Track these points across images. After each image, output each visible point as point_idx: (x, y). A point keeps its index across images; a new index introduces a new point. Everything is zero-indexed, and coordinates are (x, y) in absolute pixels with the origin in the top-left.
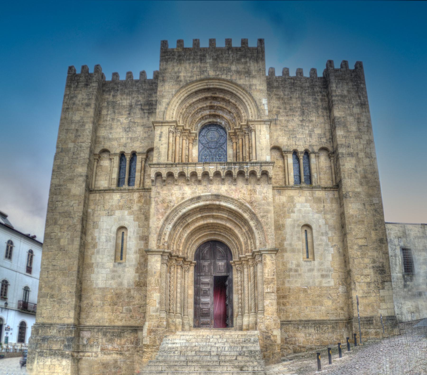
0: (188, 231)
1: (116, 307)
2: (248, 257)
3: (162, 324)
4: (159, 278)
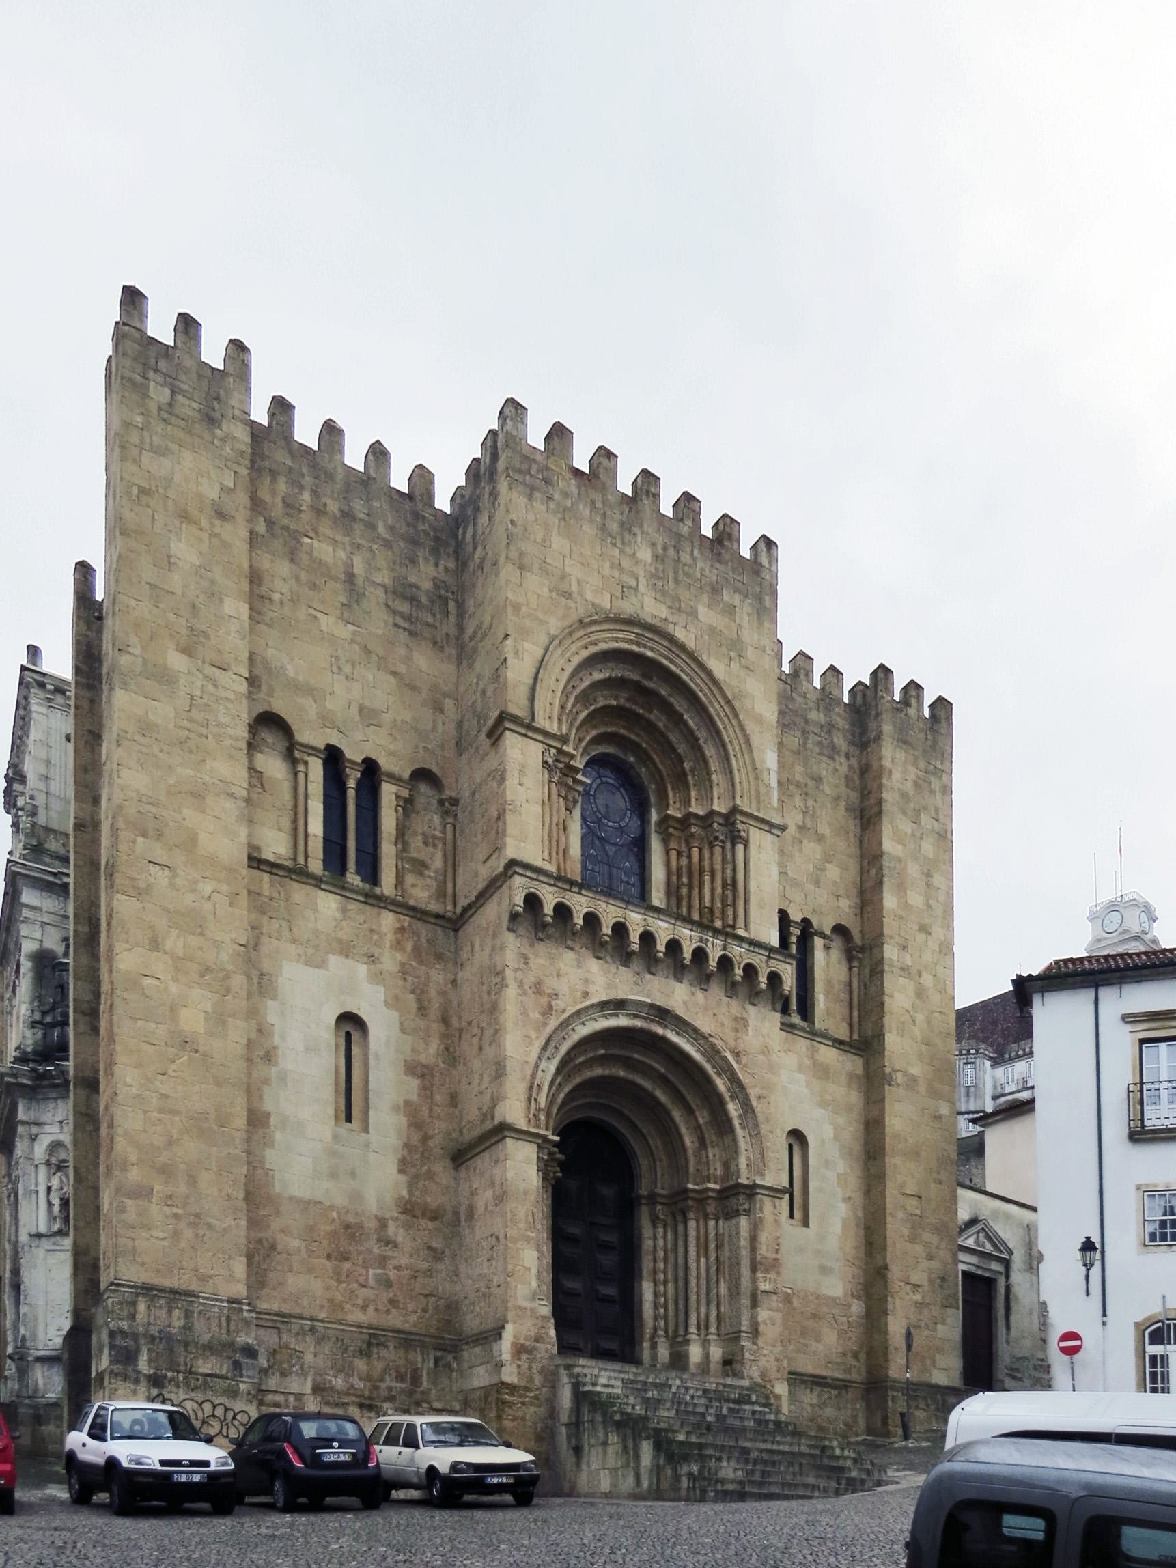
1: (347, 1266)
2: (710, 1194)
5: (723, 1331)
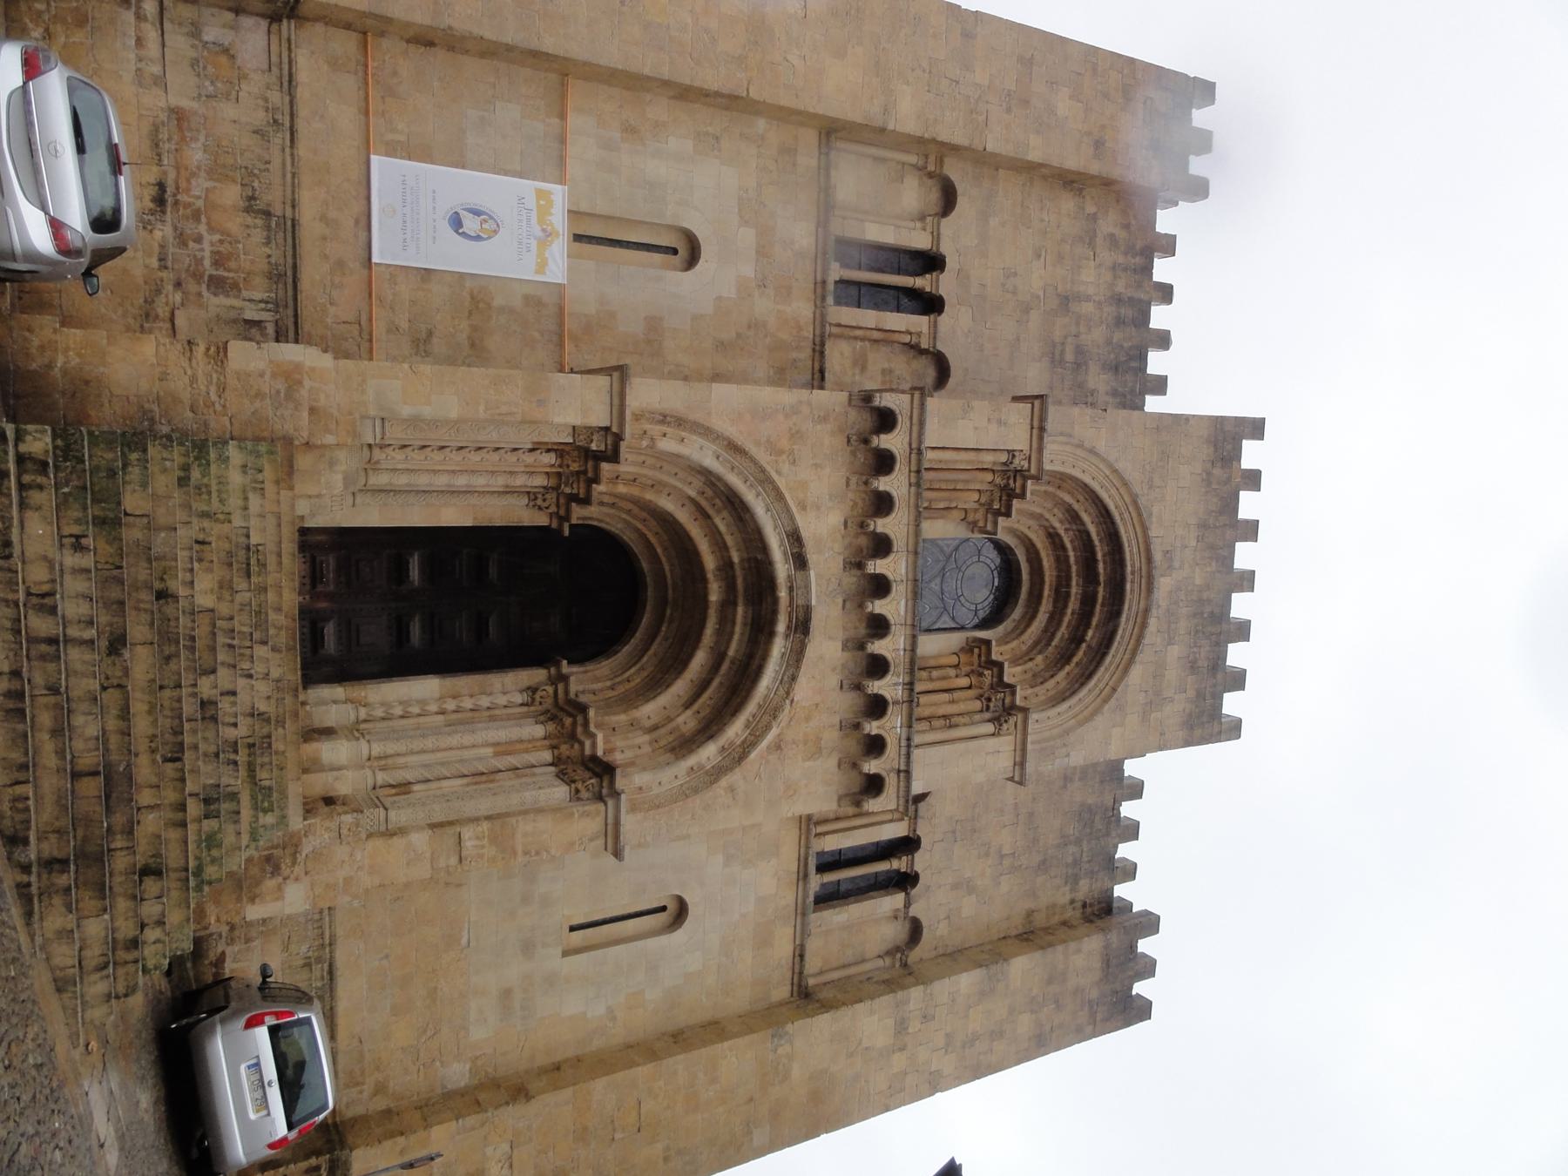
0: (683, 516)
2: (588, 744)
3: (327, 431)
4: (519, 418)
5: (381, 792)
